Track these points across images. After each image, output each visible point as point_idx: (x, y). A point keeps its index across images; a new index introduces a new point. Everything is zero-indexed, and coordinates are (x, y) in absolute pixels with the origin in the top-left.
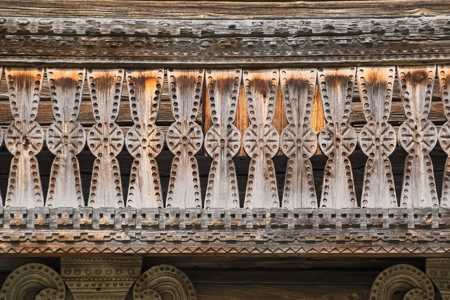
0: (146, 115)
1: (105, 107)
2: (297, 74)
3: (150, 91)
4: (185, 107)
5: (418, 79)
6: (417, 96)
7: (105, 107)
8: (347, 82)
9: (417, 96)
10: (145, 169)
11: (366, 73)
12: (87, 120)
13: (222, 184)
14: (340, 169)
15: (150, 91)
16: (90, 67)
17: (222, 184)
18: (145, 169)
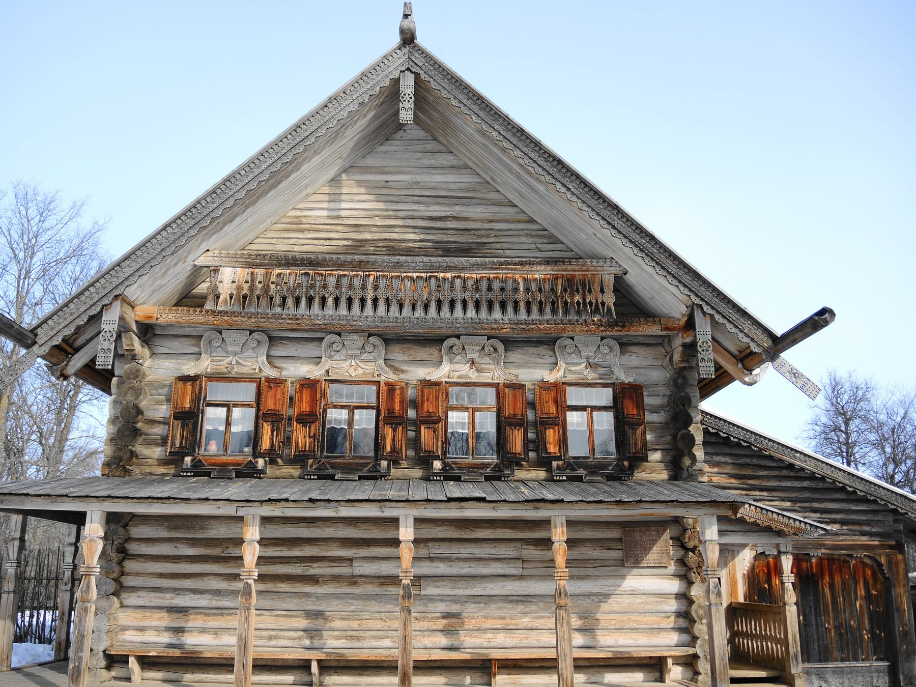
0: (370, 287)
1: (357, 282)
2: (419, 274)
3: (372, 278)
4: (382, 284)
5: (459, 277)
6: (458, 282)
7: (357, 282)
8: (436, 277)
9: (458, 282)
10: (369, 303)
11: (441, 275)
12: (351, 287)
13: (394, 309)
14: (433, 305)
15: (372, 278)
16: (352, 271)
17: (394, 309)
18: (369, 303)
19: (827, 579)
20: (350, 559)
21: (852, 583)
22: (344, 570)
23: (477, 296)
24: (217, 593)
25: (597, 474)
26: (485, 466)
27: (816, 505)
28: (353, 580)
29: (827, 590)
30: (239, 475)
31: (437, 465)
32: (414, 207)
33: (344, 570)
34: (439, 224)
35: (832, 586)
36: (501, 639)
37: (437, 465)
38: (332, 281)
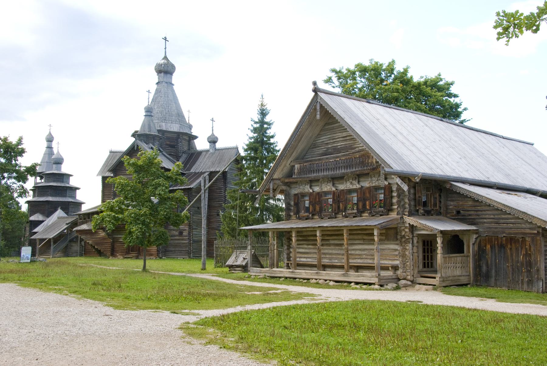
4: (325, 164)
19: (509, 246)
20: (329, 240)
21: (520, 249)
22: (328, 243)
23: (344, 164)
24: (306, 248)
25: (378, 214)
26: (353, 213)
27: (503, 216)
28: (329, 245)
29: (509, 251)
30: (306, 219)
31: (344, 214)
32: (339, 134)
33: (328, 243)
34: (345, 139)
35: (511, 249)
36: (359, 261)
37: (344, 214)
38: (315, 165)
